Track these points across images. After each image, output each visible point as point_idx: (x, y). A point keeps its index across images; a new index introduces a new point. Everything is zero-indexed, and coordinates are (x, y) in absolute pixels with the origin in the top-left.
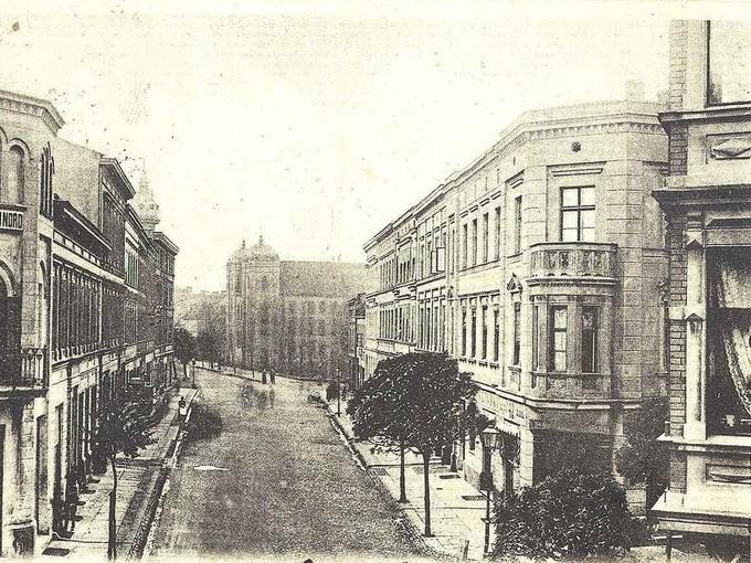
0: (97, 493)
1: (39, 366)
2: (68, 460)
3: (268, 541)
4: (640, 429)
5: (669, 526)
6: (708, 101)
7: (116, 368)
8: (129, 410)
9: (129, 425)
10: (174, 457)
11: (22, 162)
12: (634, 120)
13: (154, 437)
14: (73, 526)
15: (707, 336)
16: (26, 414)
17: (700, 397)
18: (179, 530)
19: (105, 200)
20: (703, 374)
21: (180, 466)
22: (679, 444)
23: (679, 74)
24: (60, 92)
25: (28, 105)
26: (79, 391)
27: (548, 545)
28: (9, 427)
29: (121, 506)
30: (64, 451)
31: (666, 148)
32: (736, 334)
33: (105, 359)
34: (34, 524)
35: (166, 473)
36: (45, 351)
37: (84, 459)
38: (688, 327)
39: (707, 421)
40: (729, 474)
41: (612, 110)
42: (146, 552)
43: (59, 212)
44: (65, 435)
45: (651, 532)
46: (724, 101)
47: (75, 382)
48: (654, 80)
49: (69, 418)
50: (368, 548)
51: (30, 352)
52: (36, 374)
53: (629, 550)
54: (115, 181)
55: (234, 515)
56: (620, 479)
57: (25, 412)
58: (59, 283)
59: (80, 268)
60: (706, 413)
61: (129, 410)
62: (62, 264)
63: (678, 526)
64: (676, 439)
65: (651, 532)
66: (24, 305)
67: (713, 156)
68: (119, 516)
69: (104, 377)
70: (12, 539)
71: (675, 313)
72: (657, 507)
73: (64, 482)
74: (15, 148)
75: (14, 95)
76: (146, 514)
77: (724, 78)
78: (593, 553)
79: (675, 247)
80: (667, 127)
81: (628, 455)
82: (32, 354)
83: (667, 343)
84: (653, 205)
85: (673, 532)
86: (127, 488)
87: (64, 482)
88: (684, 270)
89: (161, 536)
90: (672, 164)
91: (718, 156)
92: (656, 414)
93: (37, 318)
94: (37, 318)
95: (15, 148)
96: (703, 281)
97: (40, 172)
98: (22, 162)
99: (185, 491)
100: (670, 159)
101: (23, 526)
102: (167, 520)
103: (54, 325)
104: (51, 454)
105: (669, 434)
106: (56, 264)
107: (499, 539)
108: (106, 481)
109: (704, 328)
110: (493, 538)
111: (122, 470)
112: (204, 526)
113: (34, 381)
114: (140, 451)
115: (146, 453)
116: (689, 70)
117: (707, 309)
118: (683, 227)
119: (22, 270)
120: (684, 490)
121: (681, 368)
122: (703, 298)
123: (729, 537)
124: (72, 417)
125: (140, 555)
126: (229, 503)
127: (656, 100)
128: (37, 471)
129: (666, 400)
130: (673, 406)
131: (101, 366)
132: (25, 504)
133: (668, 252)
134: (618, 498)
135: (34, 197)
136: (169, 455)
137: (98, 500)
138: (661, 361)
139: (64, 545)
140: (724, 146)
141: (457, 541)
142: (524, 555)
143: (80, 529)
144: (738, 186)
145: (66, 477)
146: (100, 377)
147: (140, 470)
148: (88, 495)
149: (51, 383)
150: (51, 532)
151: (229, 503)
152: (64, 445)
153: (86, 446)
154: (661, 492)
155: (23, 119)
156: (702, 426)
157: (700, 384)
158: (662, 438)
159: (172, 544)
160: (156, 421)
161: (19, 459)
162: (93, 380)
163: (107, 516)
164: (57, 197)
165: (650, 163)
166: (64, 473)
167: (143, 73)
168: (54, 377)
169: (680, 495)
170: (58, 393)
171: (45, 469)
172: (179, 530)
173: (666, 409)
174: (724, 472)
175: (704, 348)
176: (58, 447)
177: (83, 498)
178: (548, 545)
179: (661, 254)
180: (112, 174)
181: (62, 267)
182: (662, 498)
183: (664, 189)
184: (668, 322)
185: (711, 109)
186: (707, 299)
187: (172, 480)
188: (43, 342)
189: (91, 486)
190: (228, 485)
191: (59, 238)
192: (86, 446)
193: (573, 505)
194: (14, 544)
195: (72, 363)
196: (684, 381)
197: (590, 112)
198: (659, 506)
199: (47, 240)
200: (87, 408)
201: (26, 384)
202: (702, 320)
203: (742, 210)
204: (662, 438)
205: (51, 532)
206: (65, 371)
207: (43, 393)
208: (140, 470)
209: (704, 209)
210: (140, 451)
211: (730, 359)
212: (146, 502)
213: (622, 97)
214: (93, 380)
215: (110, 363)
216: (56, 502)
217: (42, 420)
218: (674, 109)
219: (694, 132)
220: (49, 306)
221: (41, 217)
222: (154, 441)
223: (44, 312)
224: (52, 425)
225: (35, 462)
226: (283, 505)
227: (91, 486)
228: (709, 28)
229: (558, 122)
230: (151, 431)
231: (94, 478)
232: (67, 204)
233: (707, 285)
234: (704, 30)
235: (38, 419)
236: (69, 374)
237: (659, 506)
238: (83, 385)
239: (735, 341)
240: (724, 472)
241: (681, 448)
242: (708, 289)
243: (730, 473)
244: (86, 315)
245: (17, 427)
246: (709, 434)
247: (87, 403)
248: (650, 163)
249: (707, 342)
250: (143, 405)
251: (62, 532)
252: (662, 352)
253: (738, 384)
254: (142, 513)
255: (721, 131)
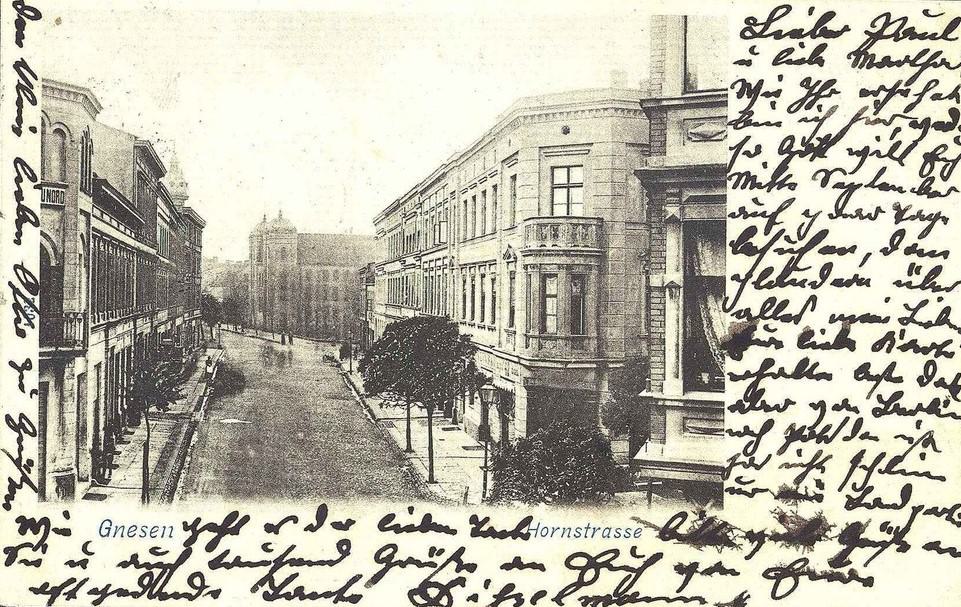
0: (132, 444)
1: (79, 329)
2: (105, 414)
3: (287, 486)
4: (623, 386)
5: (650, 473)
6: (685, 89)
7: (149, 330)
8: (161, 368)
9: (161, 382)
10: (202, 411)
11: (64, 143)
12: (618, 106)
13: (183, 393)
14: (110, 473)
15: (685, 302)
16: (67, 372)
17: (678, 357)
18: (207, 477)
19: (139, 178)
20: (681, 336)
21: (207, 419)
22: (659, 399)
23: (659, 64)
24: (98, 79)
25: (69, 92)
26: (116, 351)
27: (540, 491)
28: (52, 384)
29: (154, 456)
30: (102, 406)
31: (647, 132)
32: (711, 300)
33: (139, 322)
34: (75, 471)
35: (194, 425)
36: (84, 315)
37: (120, 412)
38: (667, 293)
39: (684, 378)
40: (704, 426)
41: (598, 97)
42: (176, 497)
43: (97, 189)
44: (103, 391)
45: (634, 479)
46: (699, 88)
47: (112, 343)
48: (637, 71)
49: (106, 376)
50: (377, 493)
51: (71, 316)
52: (77, 336)
53: (613, 495)
54: (148, 161)
55: (256, 464)
56: (605, 431)
57: (66, 370)
58: (98, 254)
59: (116, 240)
60: (684, 371)
61: (161, 368)
62: (101, 236)
63: (658, 473)
64: (656, 395)
65: (634, 479)
66: (66, 273)
67: (689, 139)
68: (152, 464)
69: (138, 339)
70: (55, 485)
71: (655, 281)
72: (639, 456)
73: (102, 434)
74: (58, 131)
75: (56, 82)
76: (176, 463)
77: (700, 68)
78: (581, 498)
79: (655, 220)
80: (648, 112)
81: (612, 409)
82: (73, 318)
83: (648, 308)
84: (635, 182)
85: (653, 479)
86: (159, 439)
87: (102, 434)
88: (663, 242)
89: (189, 483)
90: (653, 145)
91: (694, 139)
92: (638, 372)
93: (78, 286)
94: (78, 286)
95: (58, 131)
96: (681, 252)
97: (80, 153)
98: (64, 143)
99: (212, 441)
100: (650, 141)
101: (65, 474)
102: (195, 468)
103: (93, 291)
104: (90, 408)
105: (650, 390)
106: (94, 237)
107: (496, 485)
108: (140, 432)
109: (682, 294)
110: (490, 484)
111: (154, 422)
112: (229, 473)
113: (75, 342)
114: (170, 405)
115: (176, 408)
116: (668, 61)
117: (685, 277)
118: (663, 202)
119: (64, 241)
120: (663, 441)
121: (661, 330)
122: (681, 267)
123: (705, 484)
124: (109, 375)
125: (171, 500)
126: (252, 453)
127: (638, 87)
128: (78, 424)
129: (647, 359)
130: (653, 365)
131: (135, 328)
132: (67, 454)
133: (649, 226)
134: (604, 448)
135: (75, 176)
136: (197, 409)
137: (132, 450)
138: (643, 324)
139: (101, 491)
140: (699, 130)
141: (458, 487)
142: (519, 500)
143: (117, 476)
144: (712, 165)
145: (104, 429)
146: (135, 338)
147: (171, 423)
148: (124, 446)
149: (90, 344)
150: (90, 479)
151: (252, 453)
152: (102, 401)
153: (122, 401)
154: (642, 443)
155: (65, 105)
156: (680, 383)
157: (677, 345)
158: (644, 394)
159: (200, 490)
160: (185, 378)
161: (61, 413)
162: (128, 341)
163: (141, 464)
164: (95, 175)
165: (632, 145)
166: (102, 426)
167: (173, 63)
168: (93, 338)
169: (661, 446)
170: (96, 353)
171: (85, 422)
172: (207, 477)
173: (646, 367)
174: (700, 425)
175: (681, 312)
176: (97, 402)
177: (119, 448)
178: (540, 491)
179: (642, 227)
180: (145, 154)
181: (100, 239)
182: (643, 448)
183: (646, 168)
184: (649, 289)
185: (687, 95)
186: (684, 268)
187: (200, 431)
188: (83, 307)
189: (126, 437)
190: (250, 436)
191: (97, 213)
192: (122, 401)
193: (563, 455)
194: (57, 490)
195: (109, 326)
196: (663, 342)
197: (578, 98)
198: (641, 455)
199: (87, 215)
200: (123, 367)
201: (67, 344)
202: (679, 287)
203: (716, 187)
204: (644, 394)
205: (90, 479)
206: (132, 323)
207: (83, 353)
208: (171, 423)
209: (682, 186)
210: (170, 405)
211: (705, 322)
212: (176, 452)
213: (607, 85)
214: (128, 341)
215: (144, 327)
216: (94, 452)
217: (82, 377)
218: (654, 96)
219: (673, 117)
220: (89, 274)
221: (81, 194)
222: (184, 397)
223: (84, 280)
224: (91, 382)
225: (75, 415)
226: (301, 455)
227: (126, 437)
228: (686, 22)
229: (549, 107)
230: (181, 387)
231: (129, 430)
232: (105, 182)
233: (685, 255)
234: (682, 24)
235: (79, 376)
236: (107, 336)
237: (641, 455)
238: (119, 346)
239: (710, 305)
240: (700, 425)
241: (660, 403)
242: (685, 258)
243: (705, 425)
244: (121, 282)
245: (60, 383)
246: (686, 390)
247: (123, 363)
248: (632, 145)
249: (684, 306)
250: (173, 364)
251: (100, 480)
252: (643, 316)
253: (713, 345)
254: (172, 462)
255: (697, 116)
